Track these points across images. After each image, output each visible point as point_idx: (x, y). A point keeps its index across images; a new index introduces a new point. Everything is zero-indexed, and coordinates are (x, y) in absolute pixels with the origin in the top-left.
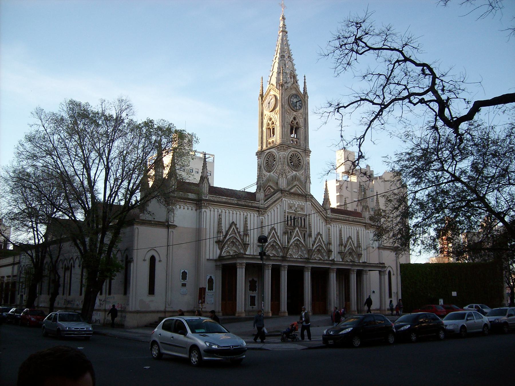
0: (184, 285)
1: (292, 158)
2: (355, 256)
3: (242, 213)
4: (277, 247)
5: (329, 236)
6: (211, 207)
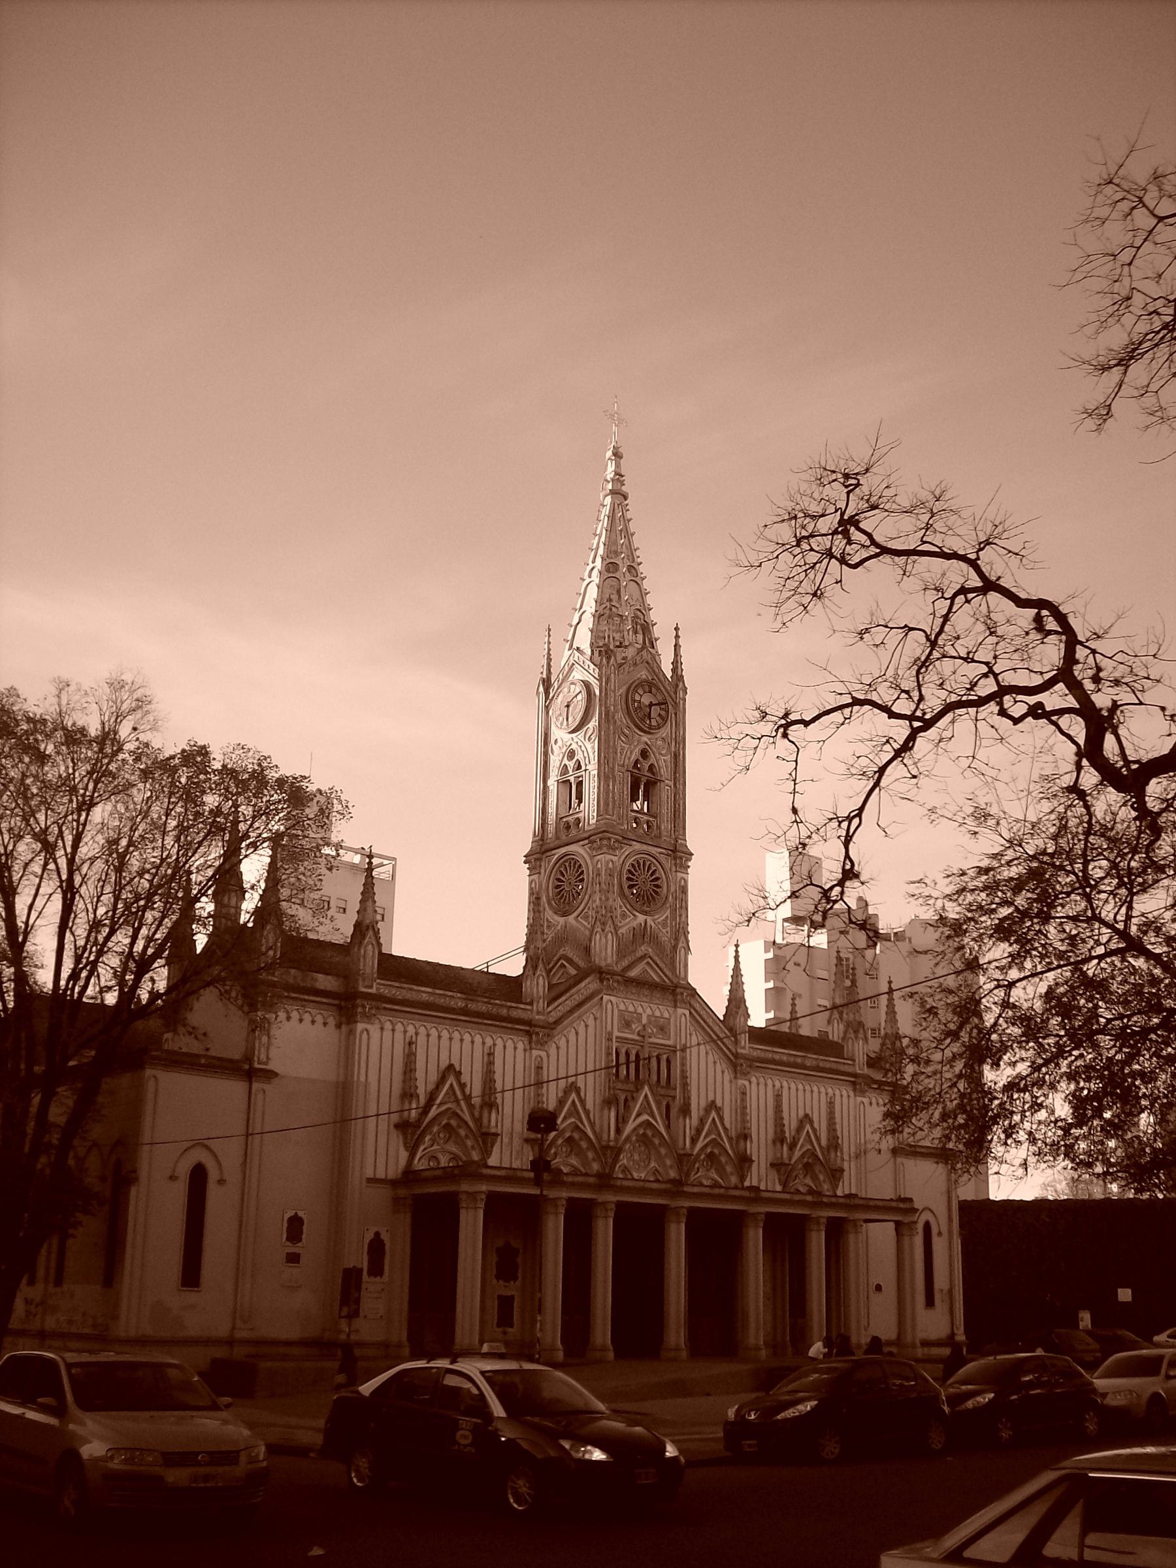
0: (293, 1258)
1: (634, 875)
2: (821, 1177)
3: (478, 1039)
4: (584, 1144)
5: (744, 1114)
6: (383, 1018)
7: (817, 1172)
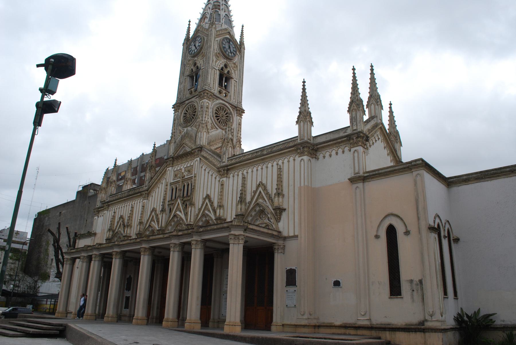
7: (267, 213)
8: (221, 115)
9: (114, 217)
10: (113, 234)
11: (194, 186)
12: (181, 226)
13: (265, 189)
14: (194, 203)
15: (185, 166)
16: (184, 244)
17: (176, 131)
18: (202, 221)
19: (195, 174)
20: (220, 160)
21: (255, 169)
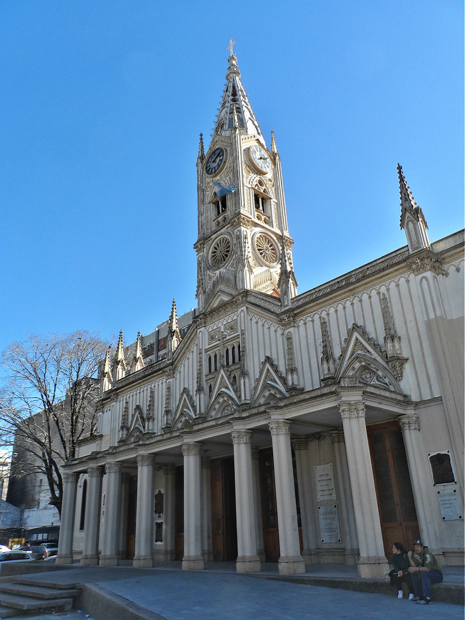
7: (374, 370)
8: (265, 248)
9: (127, 408)
10: (128, 433)
11: (244, 347)
12: (229, 408)
13: (364, 333)
14: (248, 371)
15: (225, 323)
16: (254, 431)
17: (203, 278)
18: (264, 396)
19: (242, 331)
20: (280, 304)
21: (340, 307)
